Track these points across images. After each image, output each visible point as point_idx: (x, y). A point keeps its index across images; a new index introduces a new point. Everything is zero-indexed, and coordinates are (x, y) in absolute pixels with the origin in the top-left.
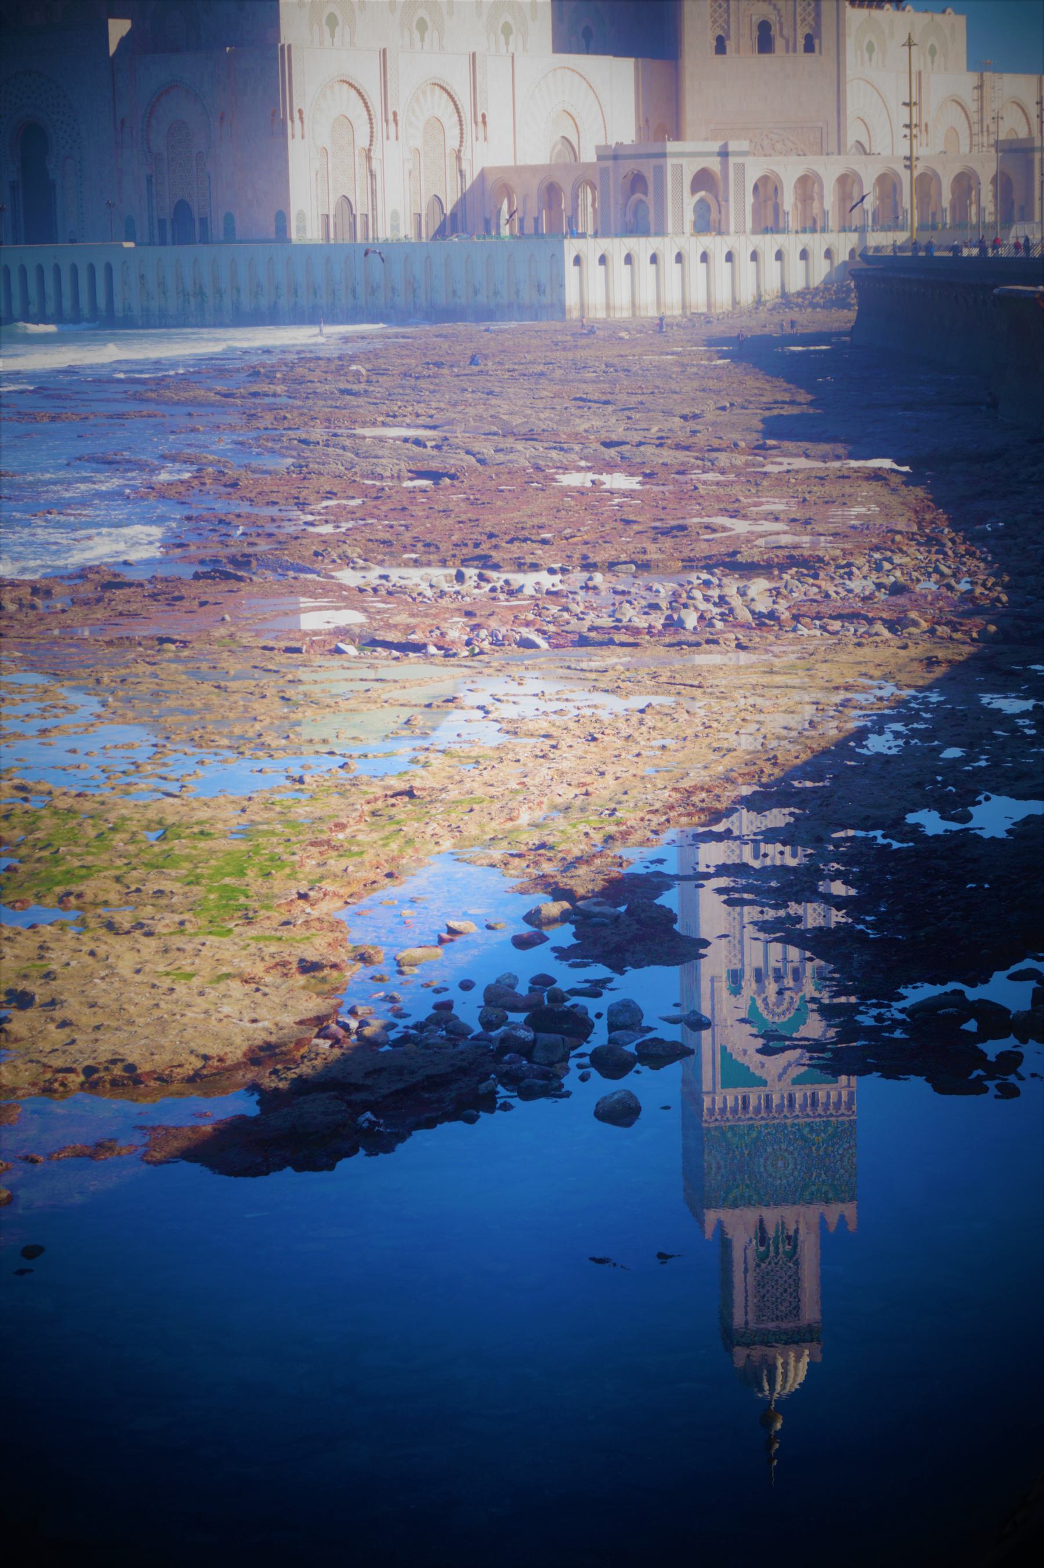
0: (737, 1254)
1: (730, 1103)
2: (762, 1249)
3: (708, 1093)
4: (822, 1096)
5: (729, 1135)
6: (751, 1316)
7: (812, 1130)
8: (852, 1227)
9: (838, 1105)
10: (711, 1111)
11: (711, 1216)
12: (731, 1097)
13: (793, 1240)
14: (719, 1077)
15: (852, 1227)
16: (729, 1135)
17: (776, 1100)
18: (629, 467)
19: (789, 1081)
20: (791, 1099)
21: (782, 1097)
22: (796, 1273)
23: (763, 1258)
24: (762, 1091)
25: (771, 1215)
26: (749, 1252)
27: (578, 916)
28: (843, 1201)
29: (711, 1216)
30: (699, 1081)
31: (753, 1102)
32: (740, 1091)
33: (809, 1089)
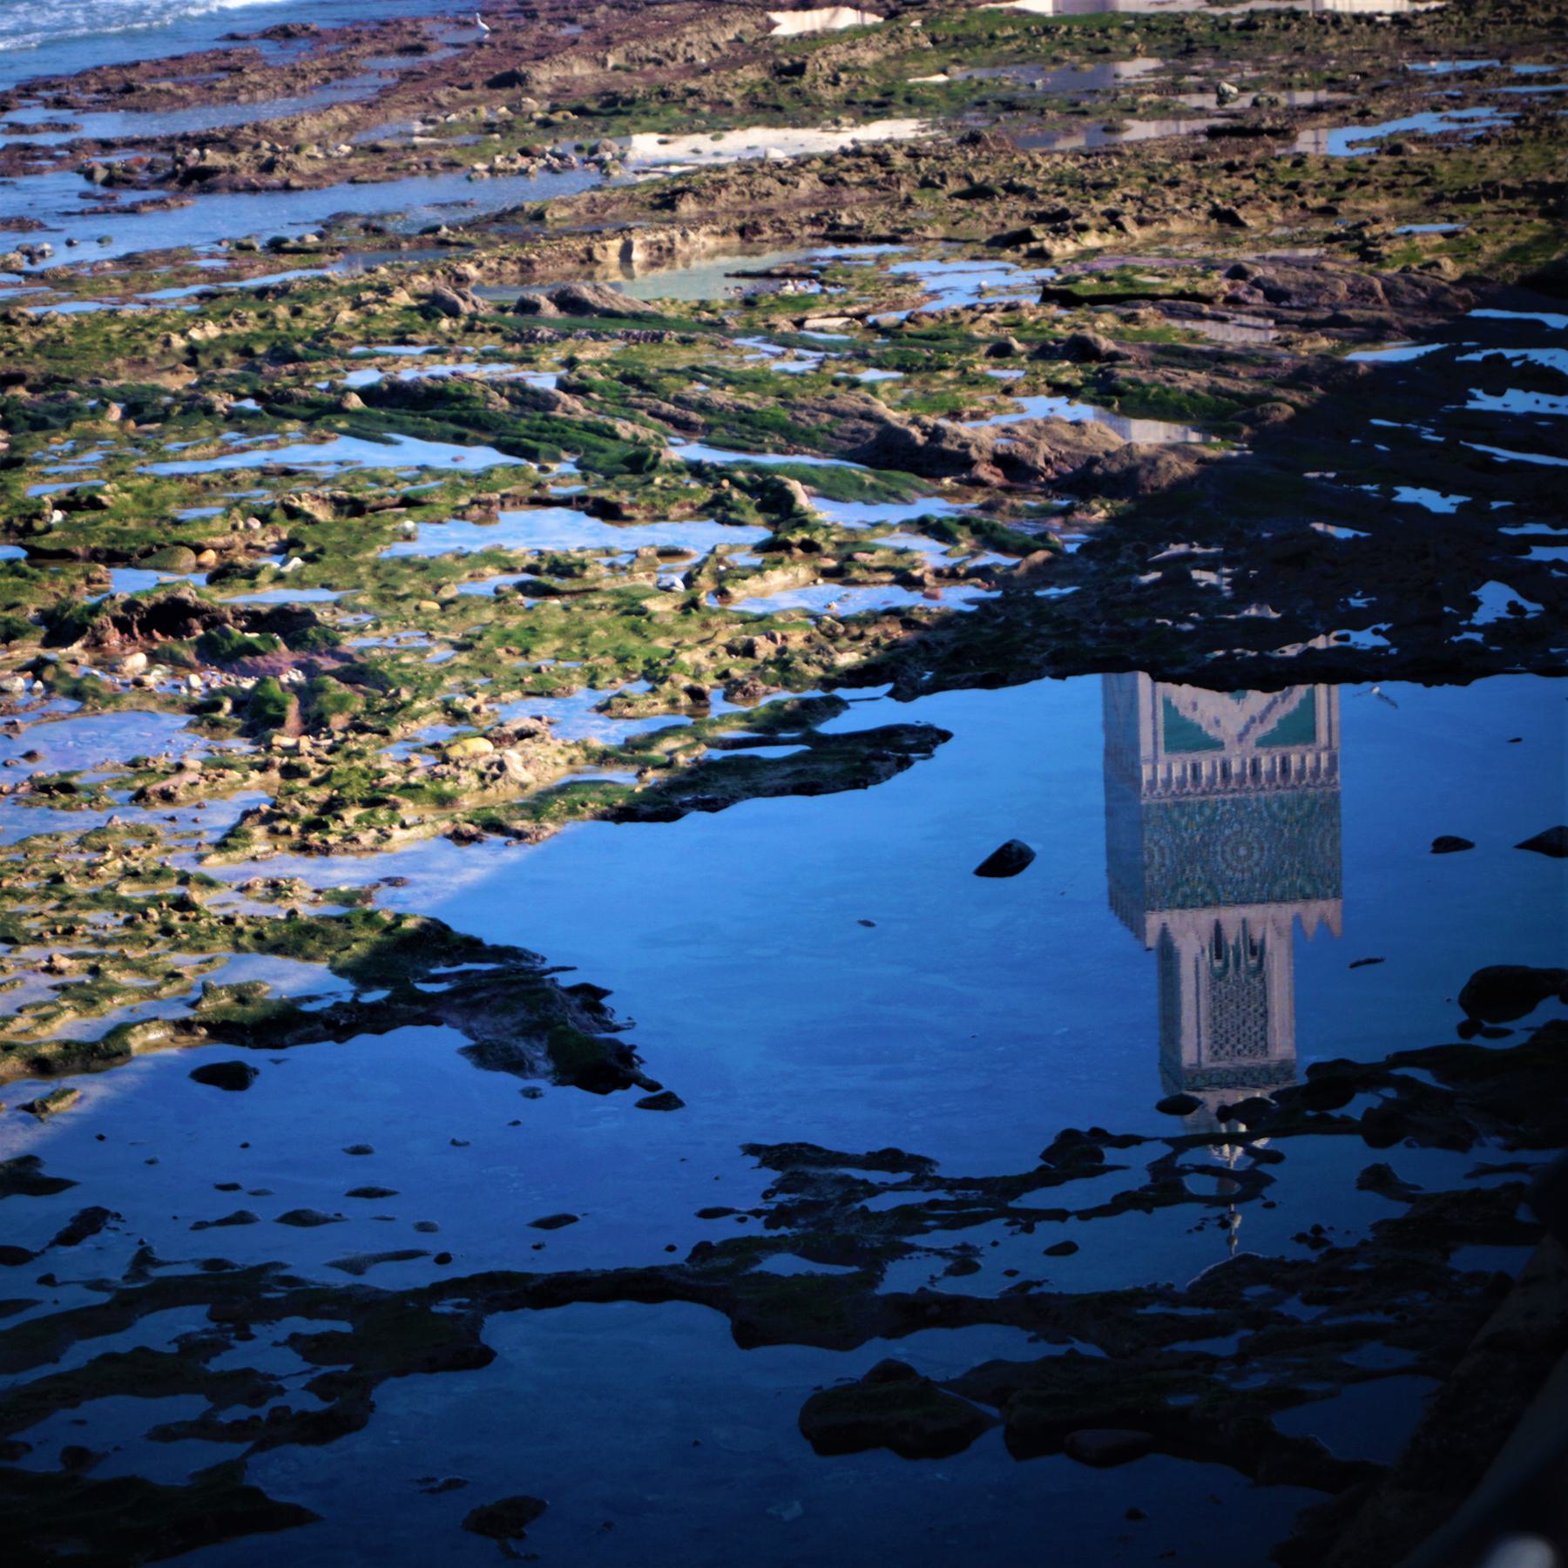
0: (1187, 969)
1: (1176, 772)
2: (1218, 964)
3: (1146, 761)
4: (1294, 760)
5: (1176, 814)
6: (1205, 1052)
7: (1282, 807)
8: (1336, 929)
9: (1316, 772)
10: (1152, 783)
11: (1154, 921)
12: (1178, 766)
13: (1257, 950)
14: (1161, 738)
15: (1336, 929)
16: (1176, 814)
17: (1235, 768)
18: (914, 103)
19: (1252, 743)
20: (1255, 764)
21: (1244, 764)
22: (1263, 1038)
23: (1219, 976)
24: (1218, 756)
25: (1231, 917)
26: (1202, 968)
27: (995, 454)
28: (1325, 897)
29: (1154, 921)
30: (1135, 747)
31: (1205, 770)
32: (1190, 758)
33: (1278, 752)
